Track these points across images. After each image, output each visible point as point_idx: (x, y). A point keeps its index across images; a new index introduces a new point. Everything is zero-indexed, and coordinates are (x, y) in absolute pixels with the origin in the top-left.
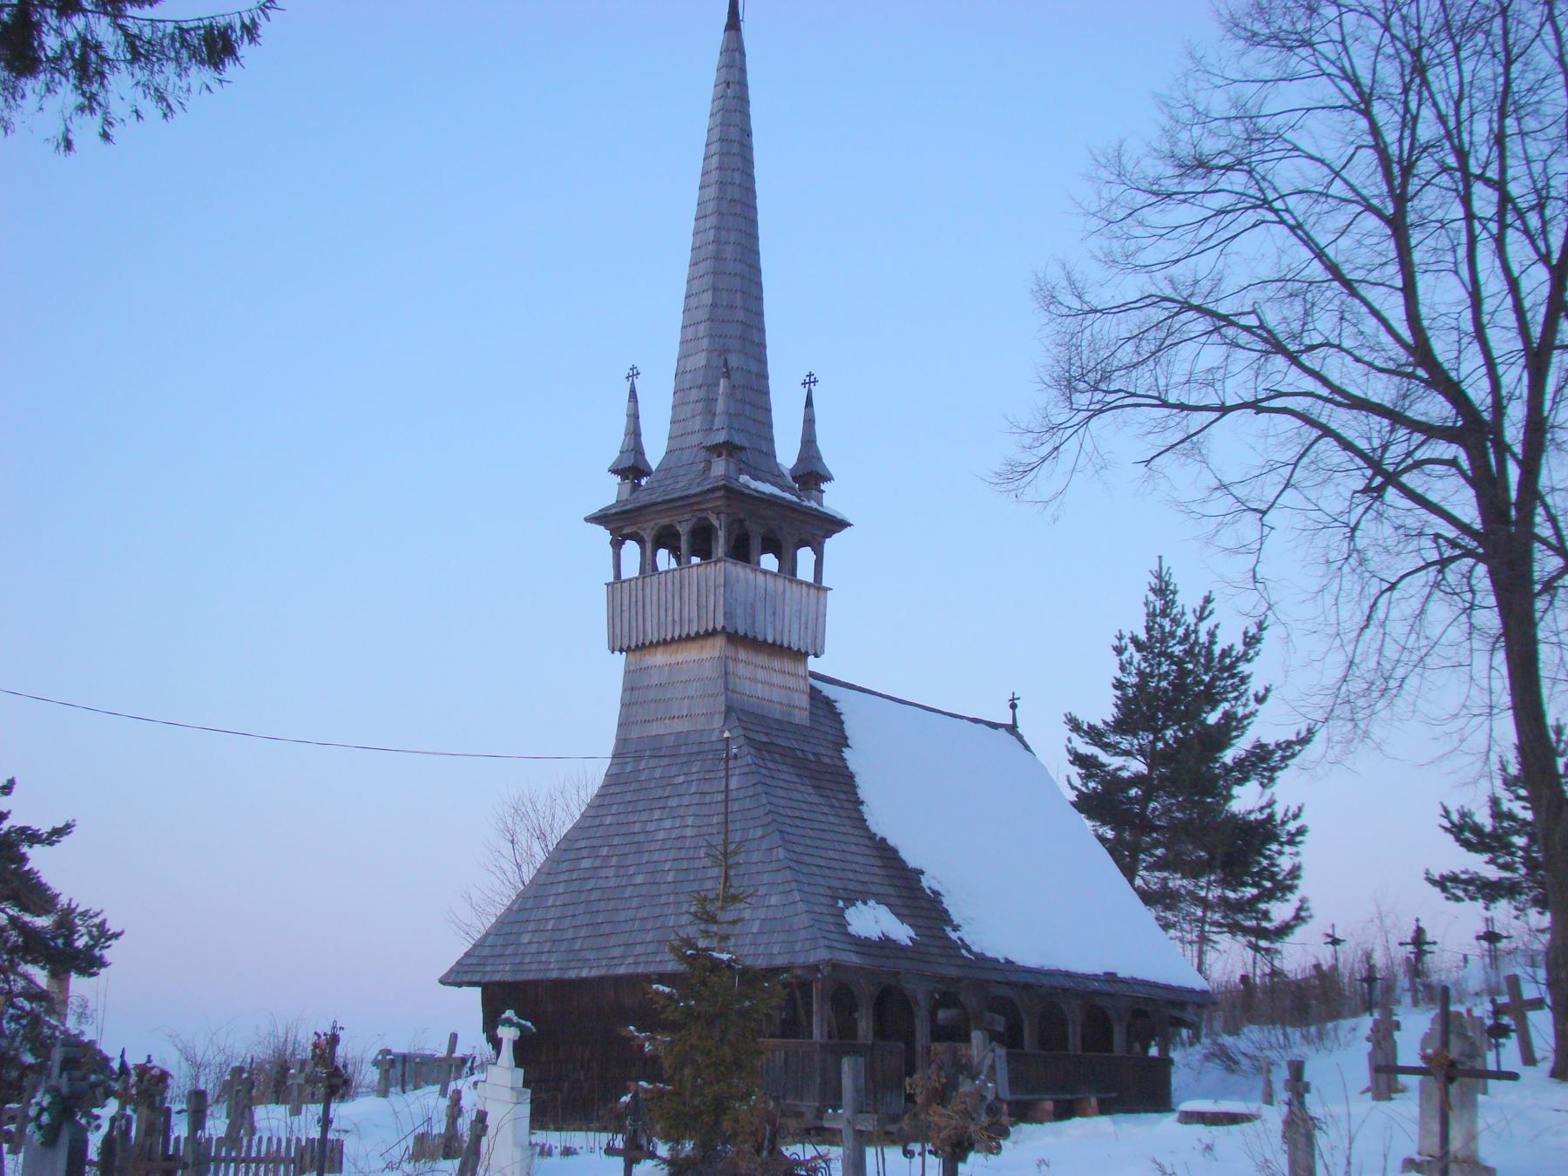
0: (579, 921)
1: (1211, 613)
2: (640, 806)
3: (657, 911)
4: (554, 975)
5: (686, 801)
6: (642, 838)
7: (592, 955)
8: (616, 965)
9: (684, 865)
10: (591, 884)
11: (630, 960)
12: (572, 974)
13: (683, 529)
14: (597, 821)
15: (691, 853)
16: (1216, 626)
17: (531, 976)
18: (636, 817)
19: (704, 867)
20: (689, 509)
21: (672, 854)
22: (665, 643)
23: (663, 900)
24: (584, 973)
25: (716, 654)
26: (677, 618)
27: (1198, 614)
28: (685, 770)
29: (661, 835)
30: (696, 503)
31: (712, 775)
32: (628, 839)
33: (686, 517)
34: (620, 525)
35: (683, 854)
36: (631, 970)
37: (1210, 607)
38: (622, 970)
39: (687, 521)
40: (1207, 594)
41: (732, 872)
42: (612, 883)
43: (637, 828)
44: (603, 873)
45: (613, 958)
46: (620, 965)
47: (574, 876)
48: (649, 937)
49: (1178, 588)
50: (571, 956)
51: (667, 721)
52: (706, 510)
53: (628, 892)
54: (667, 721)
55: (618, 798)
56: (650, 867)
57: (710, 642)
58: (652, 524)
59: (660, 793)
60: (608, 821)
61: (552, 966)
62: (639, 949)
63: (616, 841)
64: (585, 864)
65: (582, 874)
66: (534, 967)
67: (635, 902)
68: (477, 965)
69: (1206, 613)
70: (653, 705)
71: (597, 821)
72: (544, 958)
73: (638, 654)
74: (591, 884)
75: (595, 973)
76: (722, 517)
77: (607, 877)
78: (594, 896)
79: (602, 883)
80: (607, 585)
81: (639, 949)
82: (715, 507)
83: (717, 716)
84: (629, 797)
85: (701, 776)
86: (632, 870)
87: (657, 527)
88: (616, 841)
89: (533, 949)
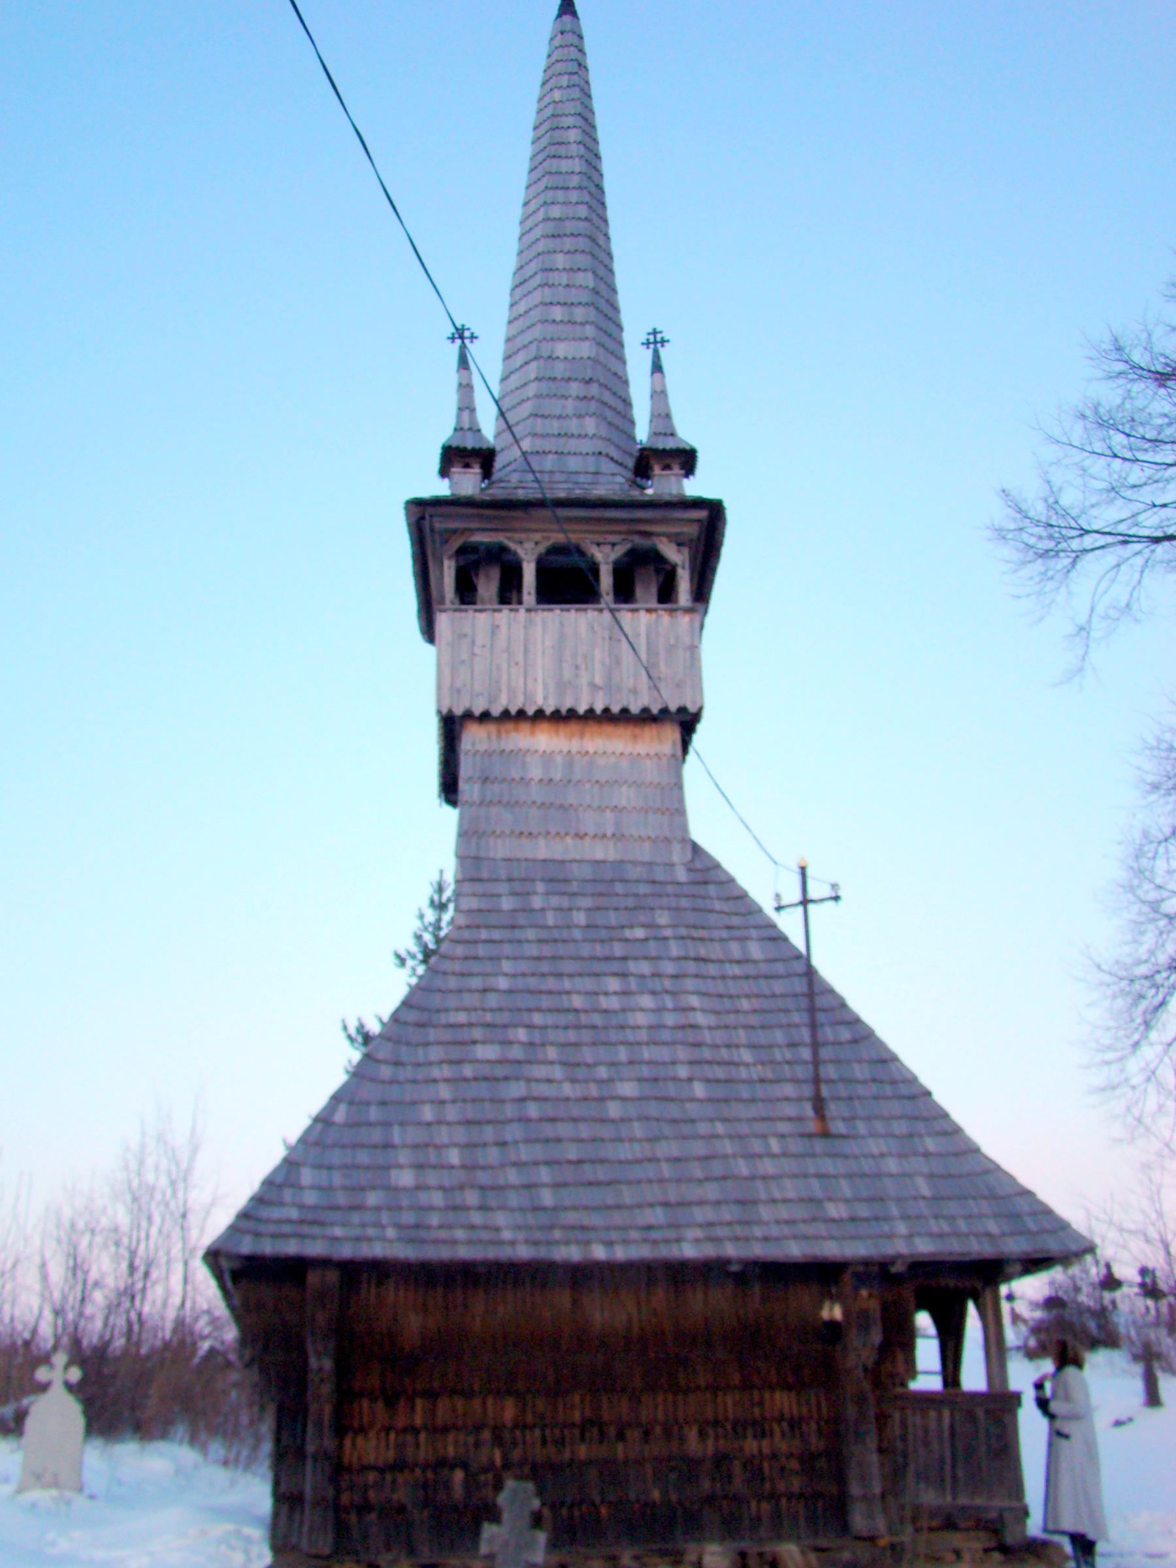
2: (569, 967)
3: (699, 1148)
4: (524, 1252)
5: (669, 968)
7: (595, 1219)
9: (720, 1072)
10: (517, 1089)
11: (699, 1233)
12: (572, 1253)
13: (605, 557)
15: (724, 1054)
17: (464, 1253)
19: (762, 1081)
20: (623, 528)
22: (563, 718)
24: (599, 1253)
28: (642, 917)
30: (632, 521)
32: (563, 1019)
33: (612, 538)
35: (707, 1054)
36: (709, 1251)
43: (577, 1001)
44: (539, 1071)
46: (678, 1240)
50: (543, 1218)
51: (569, 840)
54: (569, 840)
55: (507, 949)
56: (646, 1071)
57: (649, 732)
58: (537, 536)
60: (503, 983)
65: (486, 1070)
68: (302, 1222)
70: (533, 812)
71: (476, 983)
73: (492, 728)
74: (517, 1089)
75: (621, 1254)
84: (533, 950)
85: (683, 932)
86: (602, 1072)
88: (537, 1019)
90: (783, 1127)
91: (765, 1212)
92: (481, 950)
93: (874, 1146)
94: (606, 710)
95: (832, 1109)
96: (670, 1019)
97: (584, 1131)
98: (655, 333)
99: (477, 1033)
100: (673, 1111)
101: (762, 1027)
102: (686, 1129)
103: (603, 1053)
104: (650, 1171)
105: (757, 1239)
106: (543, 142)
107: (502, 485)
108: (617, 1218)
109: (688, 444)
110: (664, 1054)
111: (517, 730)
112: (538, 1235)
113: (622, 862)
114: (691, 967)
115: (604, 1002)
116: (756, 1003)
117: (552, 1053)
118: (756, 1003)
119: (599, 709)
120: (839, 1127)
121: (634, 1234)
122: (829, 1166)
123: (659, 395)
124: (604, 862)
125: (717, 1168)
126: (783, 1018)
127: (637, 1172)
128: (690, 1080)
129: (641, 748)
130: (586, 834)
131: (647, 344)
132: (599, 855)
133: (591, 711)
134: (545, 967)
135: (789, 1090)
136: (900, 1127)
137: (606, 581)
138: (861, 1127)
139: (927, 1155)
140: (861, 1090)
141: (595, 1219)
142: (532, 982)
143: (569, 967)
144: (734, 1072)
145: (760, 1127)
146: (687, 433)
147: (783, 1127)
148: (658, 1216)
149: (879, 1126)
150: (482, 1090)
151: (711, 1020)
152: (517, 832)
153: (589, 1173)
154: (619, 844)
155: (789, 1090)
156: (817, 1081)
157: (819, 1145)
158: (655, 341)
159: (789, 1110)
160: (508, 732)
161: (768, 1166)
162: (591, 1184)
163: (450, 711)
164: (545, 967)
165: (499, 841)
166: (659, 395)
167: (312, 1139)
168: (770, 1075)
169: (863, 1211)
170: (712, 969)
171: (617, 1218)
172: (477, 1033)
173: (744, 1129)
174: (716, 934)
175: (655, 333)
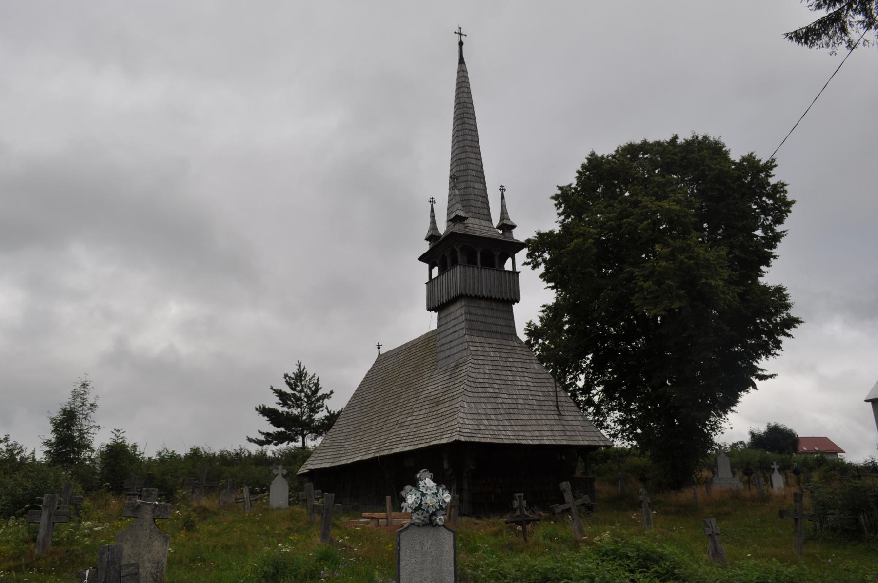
74: (500, 400)
92: (480, 362)
94: (499, 298)
95: (560, 408)
98: (502, 186)
106: (462, 111)
107: (469, 228)
109: (511, 222)
119: (493, 297)
120: (563, 413)
121: (535, 438)
123: (503, 206)
126: (544, 384)
131: (500, 189)
133: (495, 298)
137: (497, 261)
139: (579, 421)
146: (513, 218)
148: (537, 434)
150: (493, 400)
155: (551, 403)
156: (557, 401)
157: (560, 417)
158: (502, 189)
163: (462, 294)
166: (503, 206)
172: (487, 385)
175: (502, 186)
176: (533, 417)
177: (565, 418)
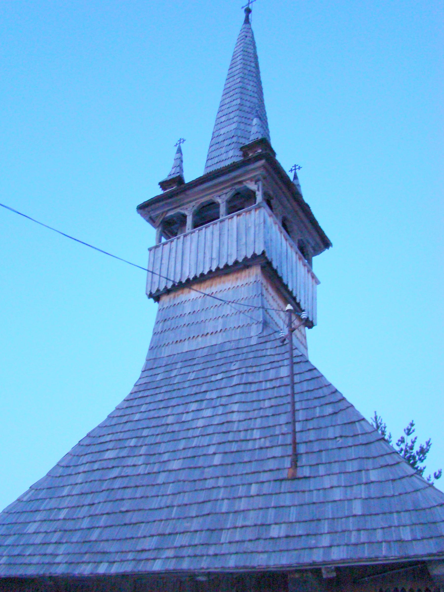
0: (98, 509)
1: (413, 431)
2: (173, 402)
3: (203, 496)
6: (176, 427)
7: (113, 547)
8: (147, 559)
9: (234, 447)
10: (115, 473)
11: (170, 553)
14: (125, 419)
15: (242, 435)
16: (416, 438)
18: (169, 411)
19: (261, 448)
21: (216, 439)
23: (209, 483)
24: (102, 569)
25: (252, 279)
26: (214, 256)
27: (406, 431)
29: (200, 423)
31: (255, 369)
34: (166, 209)
35: (230, 437)
36: (171, 565)
37: (413, 428)
38: (157, 566)
39: (226, 193)
40: (411, 422)
41: (302, 449)
42: (141, 470)
43: (170, 420)
44: (130, 461)
45: (143, 550)
46: (155, 559)
47: (96, 466)
48: (195, 525)
49: (386, 425)
52: (245, 181)
53: (161, 478)
56: (190, 453)
59: (195, 390)
61: (58, 559)
62: (180, 540)
63: (145, 432)
64: (109, 455)
65: (104, 464)
66: (36, 559)
67: (170, 489)
69: (411, 431)
70: (185, 328)
71: (125, 419)
72: (50, 549)
74: (115, 473)
75: (115, 569)
76: (260, 184)
77: (134, 466)
78: (117, 484)
79: (129, 471)
80: (150, 250)
81: (180, 540)
82: (255, 176)
83: (254, 327)
85: (243, 370)
86: (166, 457)
87: (197, 205)
88: (145, 432)
89: (39, 539)
90: (264, 477)
91: (225, 537)
93: (327, 482)
94: (218, 269)
96: (216, 420)
97: (139, 493)
99: (110, 445)
100: (196, 474)
101: (273, 415)
102: (199, 485)
103: (170, 446)
104: (164, 514)
105: (208, 555)
108: (126, 546)
110: (205, 441)
111: (182, 293)
112: (75, 559)
113: (225, 342)
114: (241, 389)
115: (185, 417)
116: (273, 402)
117: (143, 450)
118: (273, 402)
122: (287, 500)
124: (216, 345)
125: (208, 508)
127: (157, 515)
128: (215, 454)
129: (239, 283)
130: (208, 334)
132: (214, 343)
134: (162, 405)
135: (277, 452)
136: (351, 467)
138: (322, 470)
140: (330, 445)
141: (113, 547)
142: (152, 414)
143: (173, 402)
144: (244, 446)
145: (249, 478)
147: (264, 477)
149: (336, 468)
151: (242, 416)
152: (175, 341)
153: (128, 518)
154: (224, 334)
159: (272, 464)
160: (178, 295)
161: (242, 504)
162: (125, 524)
164: (162, 405)
165: (167, 347)
167: (6, 511)
168: (268, 444)
169: (299, 530)
170: (254, 387)
171: (126, 546)
173: (235, 481)
174: (263, 368)
176: (179, 500)
177: (312, 484)
